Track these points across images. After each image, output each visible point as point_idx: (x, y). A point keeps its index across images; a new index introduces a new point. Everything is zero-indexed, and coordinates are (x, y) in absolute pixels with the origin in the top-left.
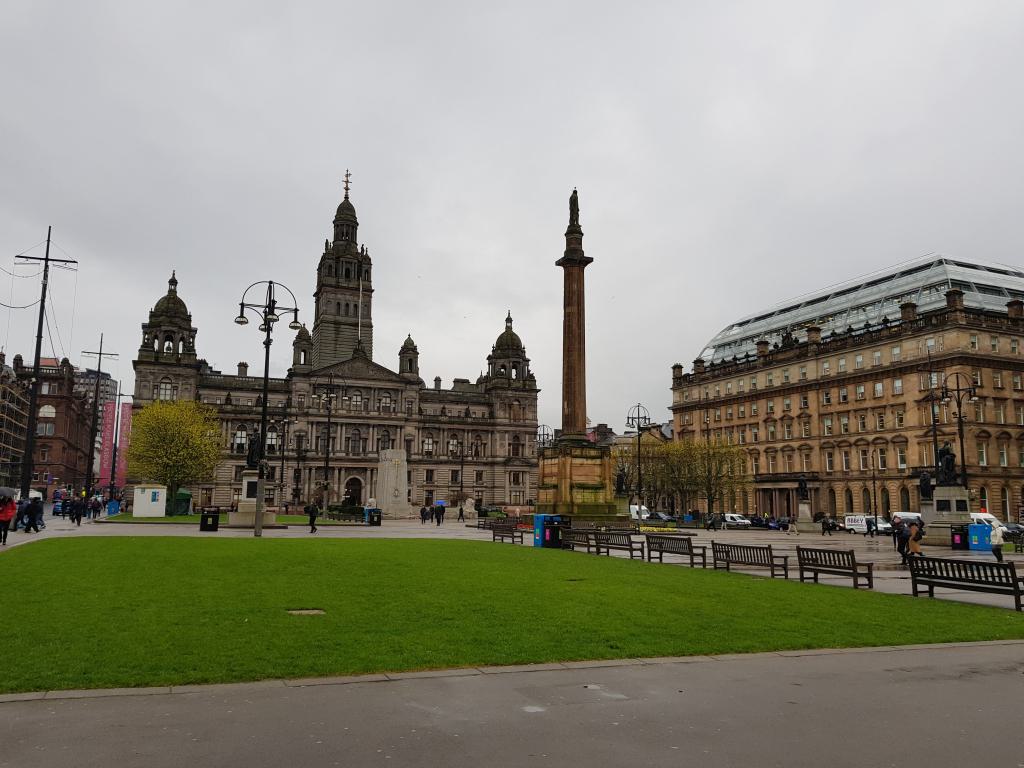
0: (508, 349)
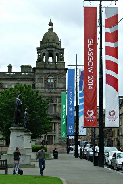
0: (50, 46)
